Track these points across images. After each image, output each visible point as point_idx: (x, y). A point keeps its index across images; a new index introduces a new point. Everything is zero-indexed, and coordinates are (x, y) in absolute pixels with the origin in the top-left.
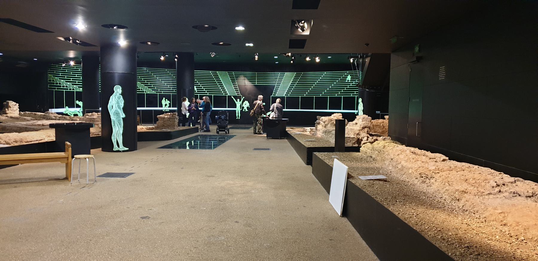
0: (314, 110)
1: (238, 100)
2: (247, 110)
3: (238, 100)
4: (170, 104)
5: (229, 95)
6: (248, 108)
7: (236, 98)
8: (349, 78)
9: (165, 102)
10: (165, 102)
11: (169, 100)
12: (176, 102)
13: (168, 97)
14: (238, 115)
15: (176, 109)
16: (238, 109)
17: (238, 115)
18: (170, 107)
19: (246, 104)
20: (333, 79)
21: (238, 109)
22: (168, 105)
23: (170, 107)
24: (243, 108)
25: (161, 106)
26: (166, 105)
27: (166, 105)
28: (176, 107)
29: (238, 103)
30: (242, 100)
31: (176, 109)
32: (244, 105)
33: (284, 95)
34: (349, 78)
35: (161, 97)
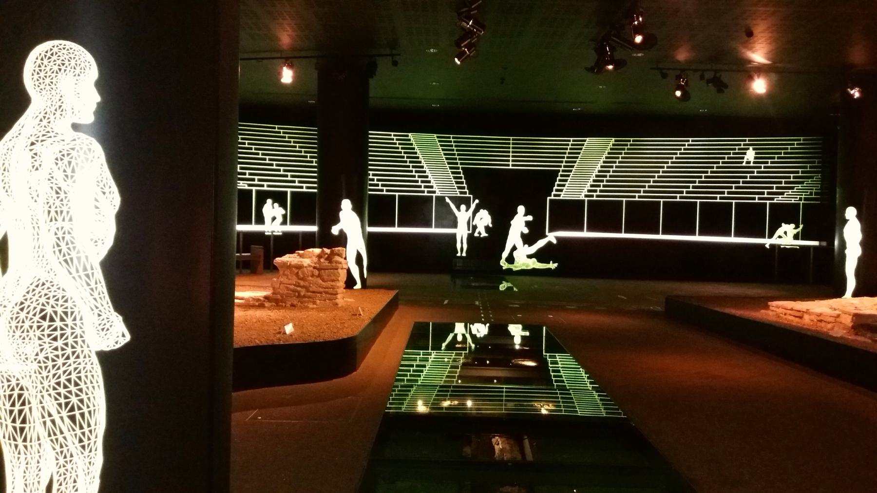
0: (697, 238)
1: (463, 207)
2: (484, 234)
3: (463, 207)
4: (285, 216)
5: (438, 194)
6: (487, 228)
7: (459, 201)
8: (750, 155)
9: (271, 210)
10: (271, 210)
11: (283, 205)
12: (315, 208)
13: (279, 198)
14: (462, 246)
15: (314, 228)
16: (461, 233)
17: (462, 246)
18: (284, 223)
19: (484, 219)
20: (710, 158)
21: (461, 233)
22: (280, 219)
23: (284, 223)
24: (475, 227)
25: (260, 220)
26: (274, 219)
27: (274, 219)
28: (312, 223)
29: (463, 215)
30: (473, 206)
31: (314, 228)
32: (477, 221)
33: (582, 197)
34: (750, 155)
35: (262, 197)
